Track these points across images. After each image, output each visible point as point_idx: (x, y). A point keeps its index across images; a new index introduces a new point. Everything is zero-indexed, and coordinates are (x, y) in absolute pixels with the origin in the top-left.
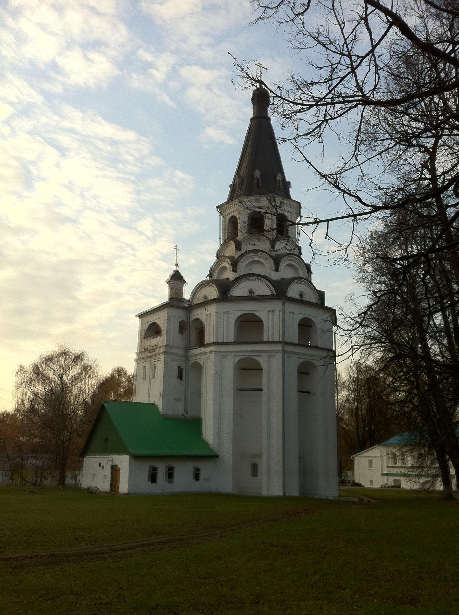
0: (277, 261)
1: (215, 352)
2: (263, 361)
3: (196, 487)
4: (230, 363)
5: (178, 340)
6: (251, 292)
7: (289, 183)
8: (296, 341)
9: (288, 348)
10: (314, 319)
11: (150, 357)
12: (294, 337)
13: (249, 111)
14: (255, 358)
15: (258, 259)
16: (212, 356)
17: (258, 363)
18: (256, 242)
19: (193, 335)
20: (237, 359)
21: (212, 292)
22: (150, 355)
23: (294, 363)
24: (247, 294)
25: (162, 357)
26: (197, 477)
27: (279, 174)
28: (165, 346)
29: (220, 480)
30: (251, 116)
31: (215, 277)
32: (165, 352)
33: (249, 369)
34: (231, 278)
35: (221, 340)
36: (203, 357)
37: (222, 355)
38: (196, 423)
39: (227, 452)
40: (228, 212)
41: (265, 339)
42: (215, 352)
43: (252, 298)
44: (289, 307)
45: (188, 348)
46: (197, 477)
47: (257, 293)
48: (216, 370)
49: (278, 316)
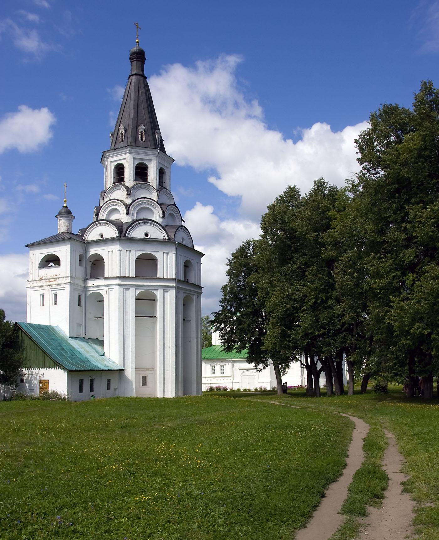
1: (120, 285)
2: (159, 294)
4: (132, 294)
5: (80, 272)
6: (146, 235)
10: (192, 261)
16: (117, 287)
17: (155, 295)
20: (138, 291)
22: (48, 283)
24: (143, 236)
25: (68, 287)
28: (70, 277)
32: (70, 283)
35: (122, 275)
36: (106, 289)
37: (126, 288)
41: (159, 275)
42: (120, 285)
43: (146, 240)
45: (85, 280)
47: (152, 236)
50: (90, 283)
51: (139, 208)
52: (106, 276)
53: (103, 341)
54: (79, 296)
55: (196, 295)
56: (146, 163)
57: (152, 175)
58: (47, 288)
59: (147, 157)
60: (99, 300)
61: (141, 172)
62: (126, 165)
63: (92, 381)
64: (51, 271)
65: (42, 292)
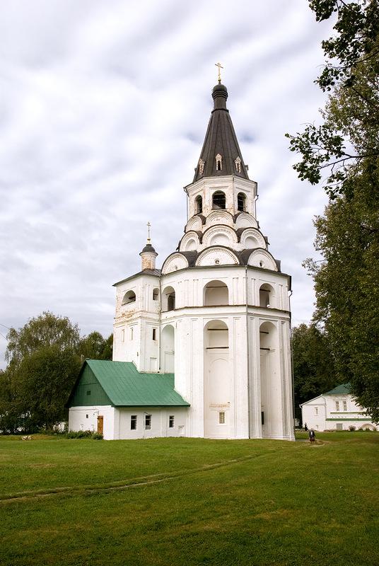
0: (239, 233)
2: (228, 322)
3: (174, 433)
4: (201, 324)
7: (247, 166)
8: (257, 303)
9: (251, 311)
11: (128, 321)
12: (256, 301)
13: (210, 107)
14: (222, 320)
15: (225, 233)
18: (219, 218)
19: (165, 301)
21: (182, 263)
22: (127, 319)
23: (256, 324)
24: (213, 264)
26: (171, 425)
27: (238, 158)
29: (193, 427)
30: (212, 109)
31: (183, 249)
33: (216, 329)
34: (199, 251)
36: (176, 320)
38: (170, 377)
39: (197, 403)
40: (195, 192)
44: (252, 274)
46: (171, 425)
47: (221, 263)
48: (189, 330)
49: (242, 282)
50: (164, 316)
51: (212, 236)
52: (176, 307)
53: (173, 375)
54: (154, 330)
55: (280, 321)
56: (222, 190)
57: (231, 202)
58: (126, 324)
59: (220, 185)
60: (170, 330)
61: (219, 200)
62: (203, 197)
63: (148, 417)
64: (132, 306)
65: (123, 328)
